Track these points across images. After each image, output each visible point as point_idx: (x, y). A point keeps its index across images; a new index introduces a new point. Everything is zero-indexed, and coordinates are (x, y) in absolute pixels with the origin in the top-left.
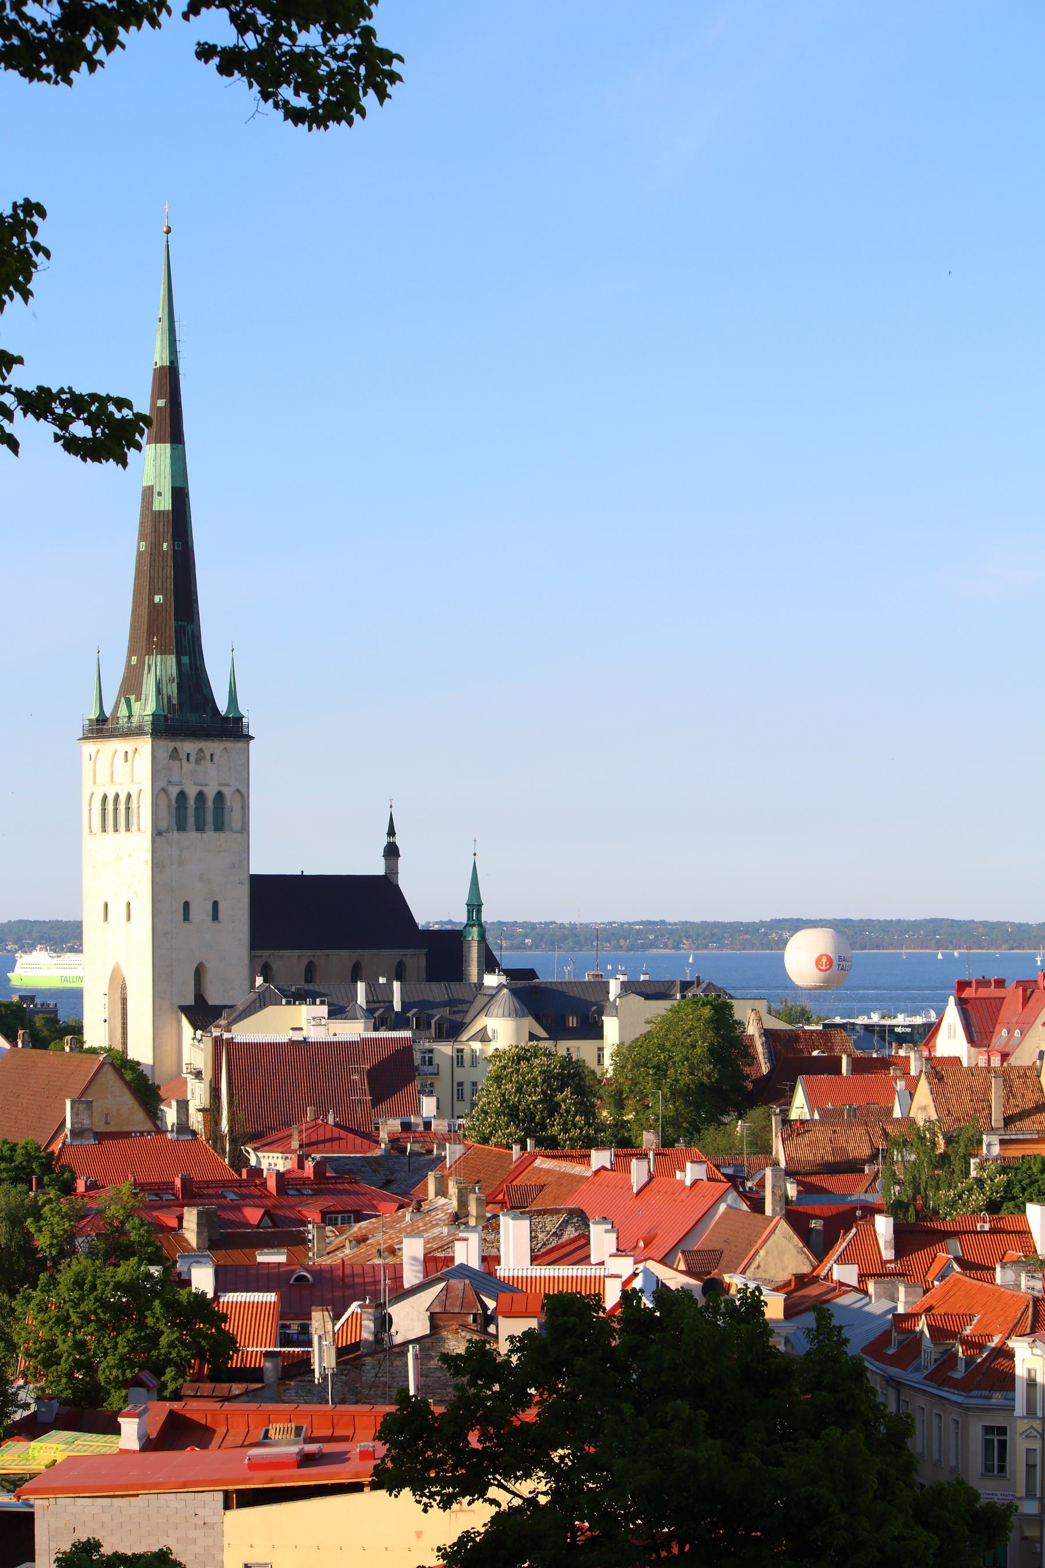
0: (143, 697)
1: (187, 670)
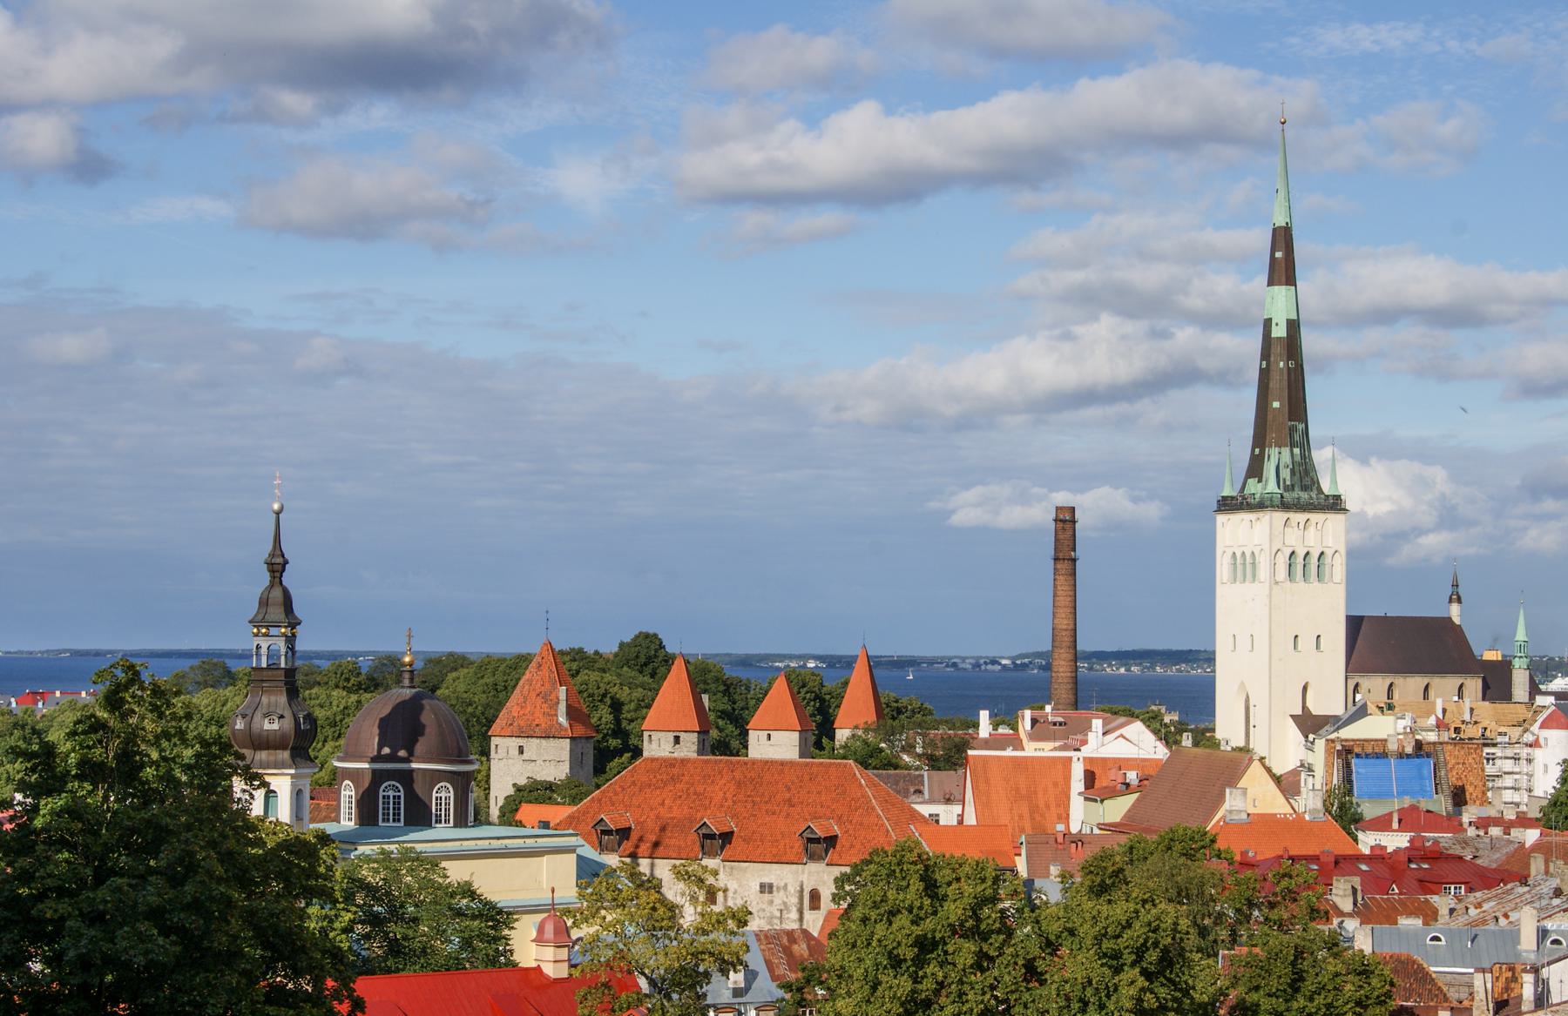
0: (1264, 479)
1: (1298, 458)
